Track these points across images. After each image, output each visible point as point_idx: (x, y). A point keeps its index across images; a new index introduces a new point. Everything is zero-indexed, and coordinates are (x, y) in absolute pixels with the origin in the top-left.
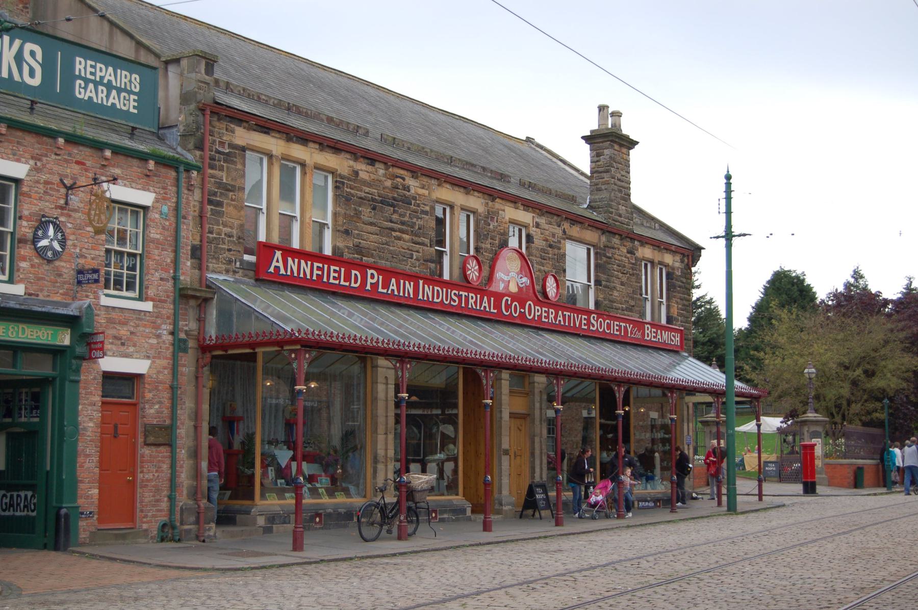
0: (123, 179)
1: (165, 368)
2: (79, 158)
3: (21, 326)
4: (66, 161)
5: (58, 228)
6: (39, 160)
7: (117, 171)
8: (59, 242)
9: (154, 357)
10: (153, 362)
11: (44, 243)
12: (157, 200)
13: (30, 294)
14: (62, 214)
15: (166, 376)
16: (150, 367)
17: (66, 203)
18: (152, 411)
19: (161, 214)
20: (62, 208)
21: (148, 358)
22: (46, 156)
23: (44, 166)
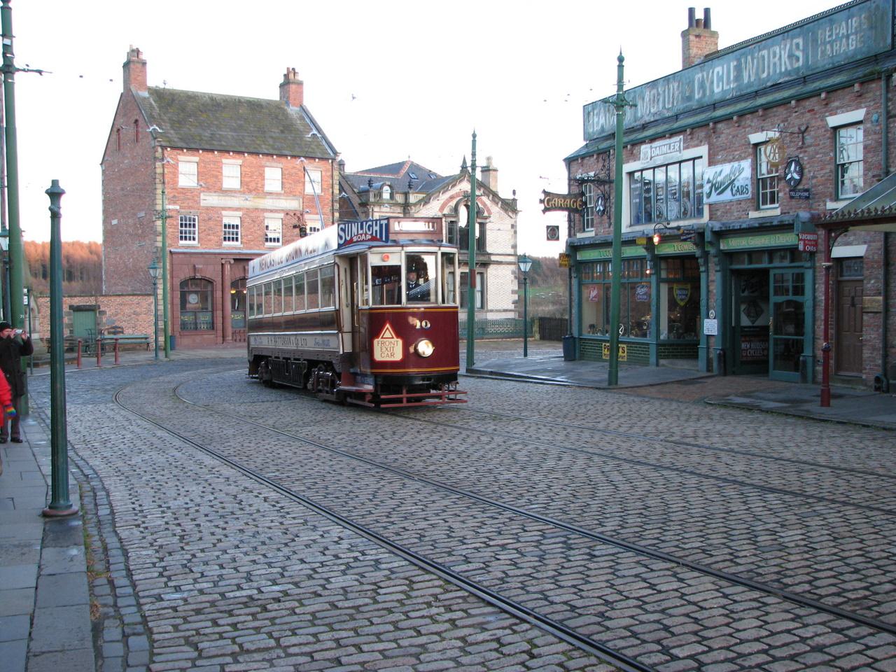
0: (841, 107)
1: (879, 249)
2: (810, 108)
3: (777, 236)
4: (803, 113)
5: (798, 163)
6: (787, 121)
7: (837, 104)
8: (797, 172)
9: (870, 242)
10: (869, 246)
11: (789, 176)
12: (867, 113)
13: (785, 213)
14: (801, 153)
15: (879, 256)
16: (867, 250)
17: (803, 143)
18: (869, 285)
19: (872, 122)
20: (801, 148)
21: (865, 243)
22: (790, 116)
23: (789, 124)
